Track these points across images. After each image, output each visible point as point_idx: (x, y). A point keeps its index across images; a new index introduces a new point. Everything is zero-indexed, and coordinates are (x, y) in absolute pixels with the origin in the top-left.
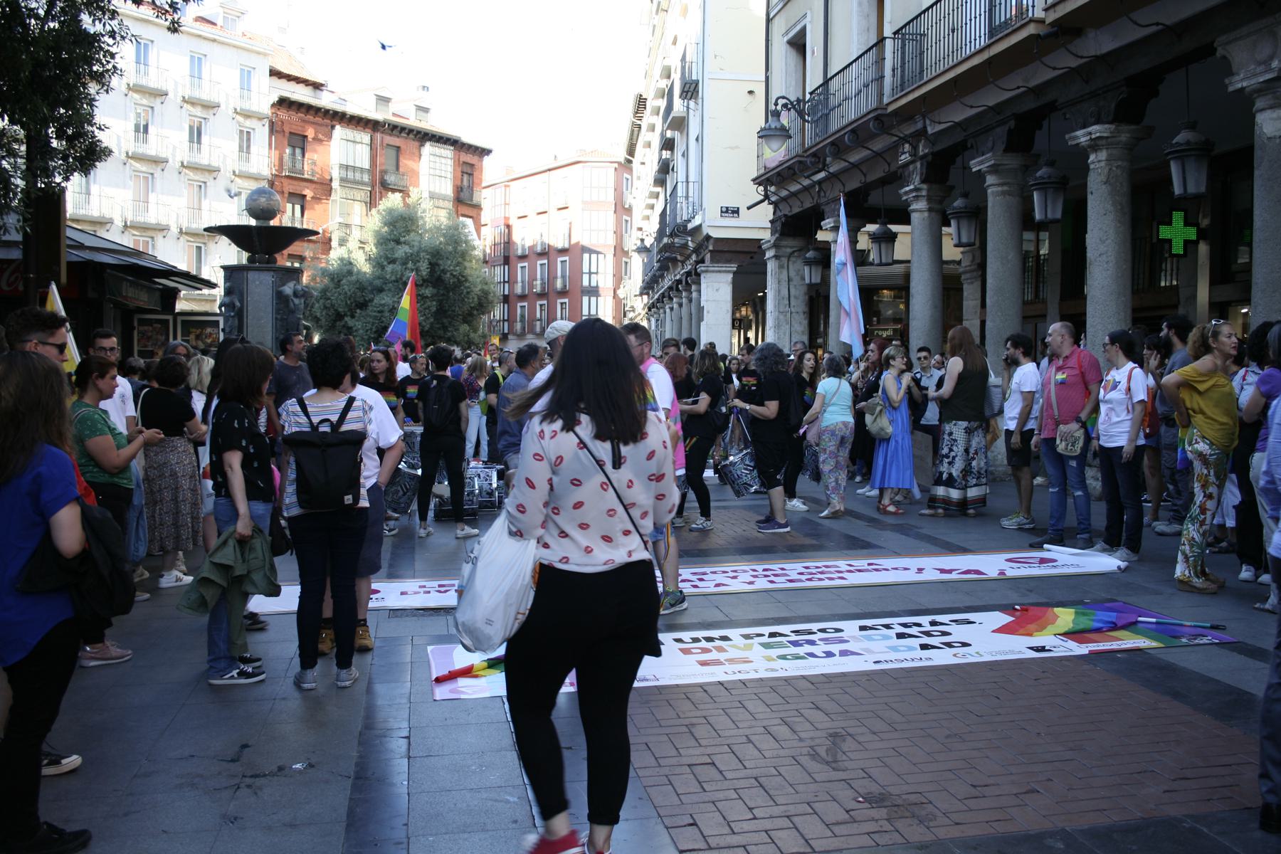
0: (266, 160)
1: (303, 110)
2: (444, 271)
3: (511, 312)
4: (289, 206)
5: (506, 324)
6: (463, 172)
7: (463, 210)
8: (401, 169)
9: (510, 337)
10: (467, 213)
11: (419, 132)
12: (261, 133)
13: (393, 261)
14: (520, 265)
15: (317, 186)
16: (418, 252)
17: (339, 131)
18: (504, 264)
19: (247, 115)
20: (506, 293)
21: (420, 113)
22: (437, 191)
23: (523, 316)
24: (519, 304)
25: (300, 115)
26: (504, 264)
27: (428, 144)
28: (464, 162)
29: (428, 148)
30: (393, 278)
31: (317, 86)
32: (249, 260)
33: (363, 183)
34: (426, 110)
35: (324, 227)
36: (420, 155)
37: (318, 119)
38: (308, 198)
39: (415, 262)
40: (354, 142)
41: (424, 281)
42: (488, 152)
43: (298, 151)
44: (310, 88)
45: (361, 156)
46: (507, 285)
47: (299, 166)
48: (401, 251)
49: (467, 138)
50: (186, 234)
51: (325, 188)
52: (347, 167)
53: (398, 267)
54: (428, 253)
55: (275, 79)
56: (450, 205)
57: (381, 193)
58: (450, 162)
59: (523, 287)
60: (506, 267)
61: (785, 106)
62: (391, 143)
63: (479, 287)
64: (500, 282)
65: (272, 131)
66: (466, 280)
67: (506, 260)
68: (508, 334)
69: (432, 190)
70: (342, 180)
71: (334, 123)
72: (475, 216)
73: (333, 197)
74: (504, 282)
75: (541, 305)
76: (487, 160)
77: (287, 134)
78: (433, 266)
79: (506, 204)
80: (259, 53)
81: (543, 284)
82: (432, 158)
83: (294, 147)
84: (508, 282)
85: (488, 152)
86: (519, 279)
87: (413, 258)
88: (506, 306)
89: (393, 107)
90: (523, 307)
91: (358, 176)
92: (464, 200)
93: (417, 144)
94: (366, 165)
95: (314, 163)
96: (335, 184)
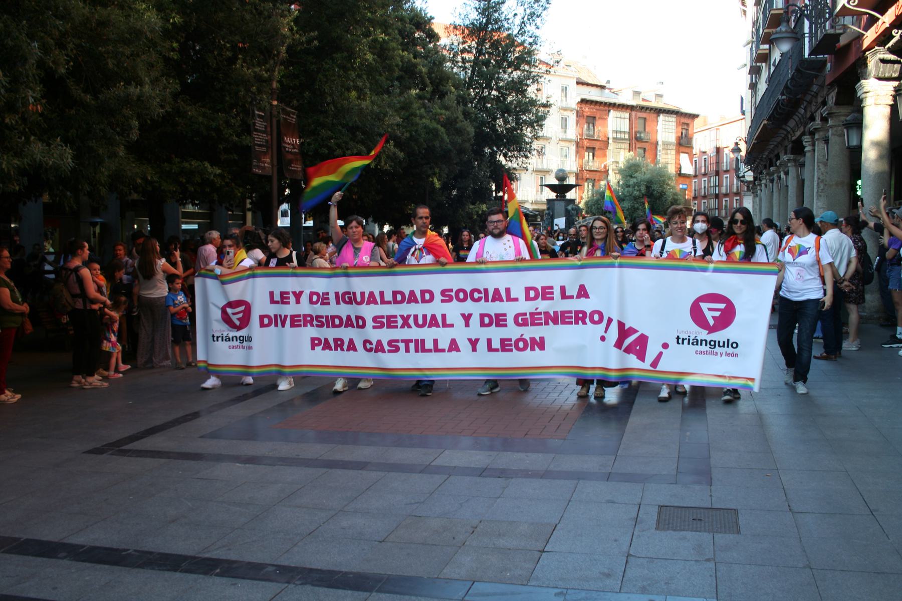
0: (575, 131)
1: (593, 104)
2: (654, 190)
3: (720, 204)
4: (586, 154)
5: (717, 211)
6: (682, 129)
7: (682, 149)
8: (646, 130)
10: (684, 151)
11: (656, 109)
12: (572, 118)
13: (628, 186)
14: (725, 176)
15: (601, 143)
16: (641, 181)
17: (613, 113)
18: (716, 176)
19: (565, 109)
20: (717, 192)
21: (660, 98)
22: (667, 140)
23: (726, 206)
24: (724, 199)
25: (592, 106)
26: (716, 176)
27: (661, 115)
28: (683, 123)
29: (662, 117)
30: (628, 194)
31: (603, 87)
33: (624, 139)
34: (661, 96)
35: (605, 163)
36: (658, 121)
37: (602, 108)
38: (596, 149)
39: (639, 186)
40: (620, 118)
41: (643, 195)
42: (697, 116)
44: (599, 88)
45: (625, 126)
47: (591, 133)
48: (632, 181)
49: (684, 109)
50: (536, 171)
52: (617, 132)
53: (631, 189)
54: (644, 181)
55: (580, 86)
56: (674, 147)
57: (635, 143)
58: (674, 124)
60: (717, 177)
61: (740, 140)
62: (641, 116)
63: (671, 197)
65: (577, 115)
66: (665, 194)
67: (717, 173)
69: (664, 140)
70: (614, 138)
71: (610, 108)
72: (689, 152)
73: (610, 147)
74: (716, 186)
75: (737, 200)
76: (696, 121)
77: (585, 117)
78: (648, 187)
79: (717, 140)
80: (571, 77)
81: (737, 187)
82: (664, 122)
83: (589, 124)
84: (718, 186)
85: (697, 116)
87: (638, 184)
88: (717, 200)
89: (642, 96)
90: (726, 201)
91: (622, 136)
92: (684, 143)
93: (655, 115)
94: (627, 130)
95: (599, 131)
96: (611, 141)
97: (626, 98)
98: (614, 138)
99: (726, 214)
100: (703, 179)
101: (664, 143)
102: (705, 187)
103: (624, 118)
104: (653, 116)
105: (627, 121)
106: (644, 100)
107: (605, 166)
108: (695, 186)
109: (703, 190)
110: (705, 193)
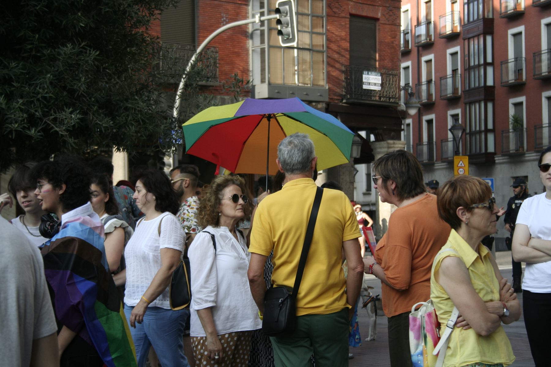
5: (491, 138)
9: (498, 159)
20: (490, 82)
24: (512, 101)
46: (490, 70)
59: (518, 71)
60: (489, 39)
64: (479, 65)
68: (494, 154)
74: (486, 64)
86: (511, 55)
88: (490, 106)
90: (518, 105)
99: (520, 140)
100: (450, 51)
102: (454, 71)
109: (450, 81)
110: (455, 89)
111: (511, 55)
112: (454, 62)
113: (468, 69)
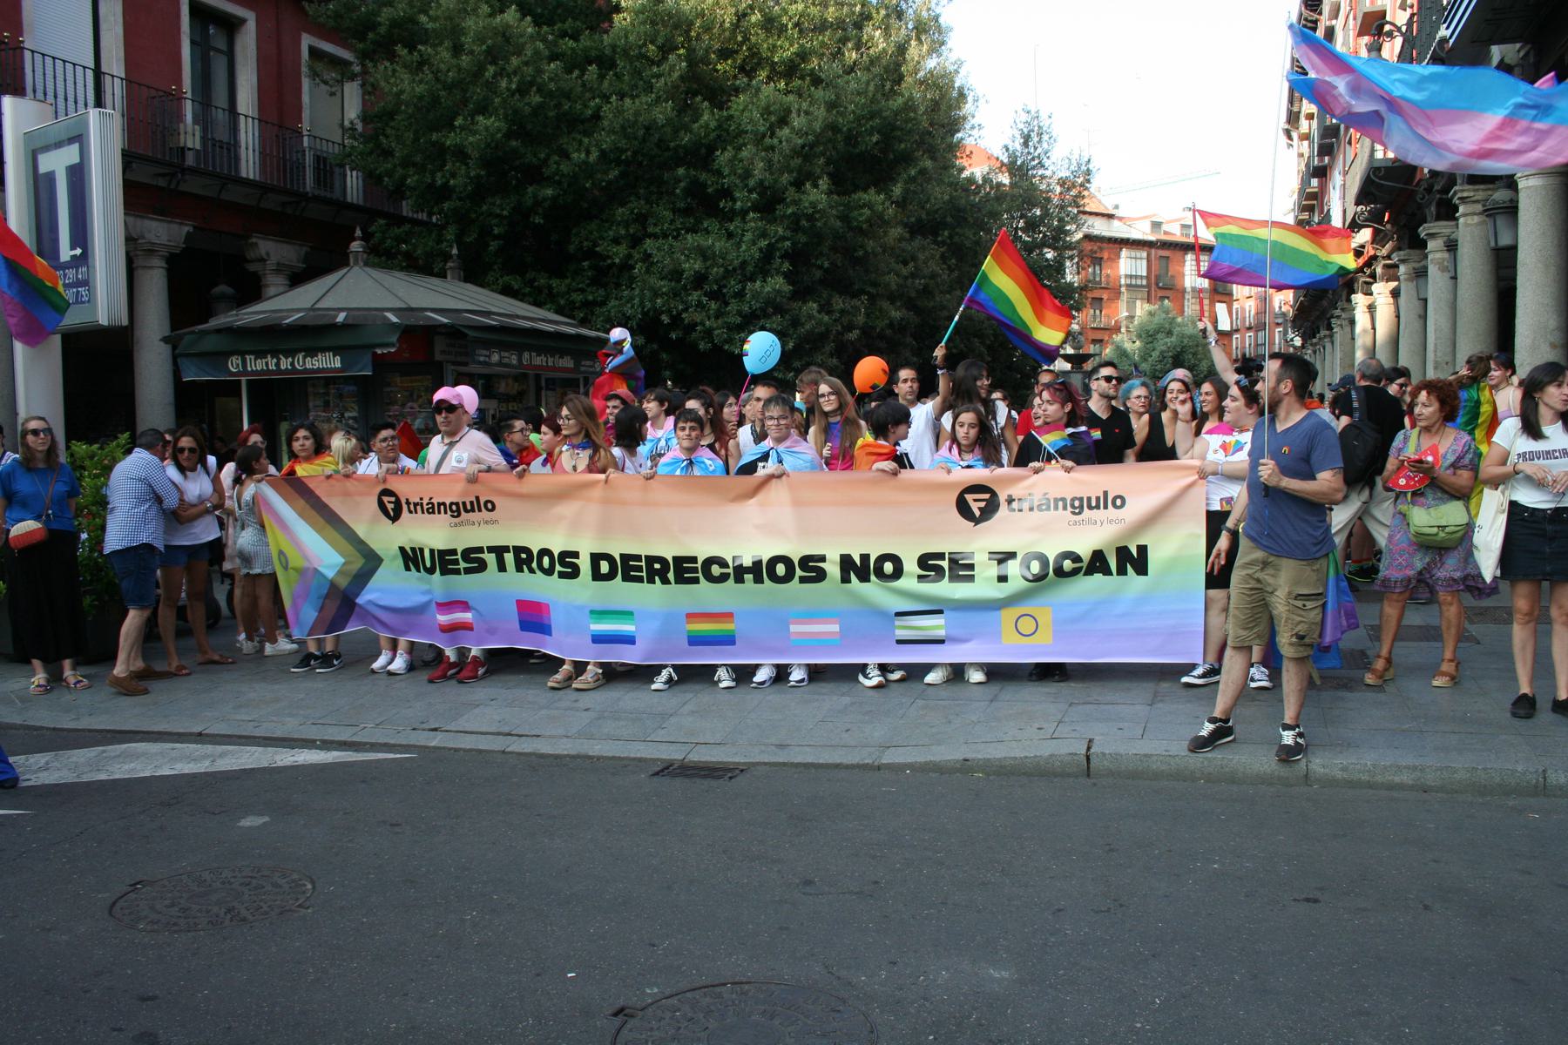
7: (1218, 297)
17: (1124, 252)
31: (1110, 217)
32: (1072, 368)
33: (1142, 286)
36: (1185, 261)
37: (1111, 245)
40: (1136, 258)
43: (1097, 268)
45: (1141, 268)
47: (1098, 279)
51: (1117, 293)
52: (1131, 277)
86: (1277, 342)
91: (1139, 282)
93: (1182, 253)
94: (1145, 274)
95: (1108, 276)
96: (1123, 289)
97: (1141, 232)
98: (1128, 286)
100: (1248, 335)
101: (1194, 289)
102: (1250, 345)
103: (1141, 258)
104: (1179, 254)
105: (1145, 262)
106: (1166, 233)
107: (1116, 322)
108: (1237, 343)
111: (1277, 342)
112: (1250, 340)
113: (1257, 345)
